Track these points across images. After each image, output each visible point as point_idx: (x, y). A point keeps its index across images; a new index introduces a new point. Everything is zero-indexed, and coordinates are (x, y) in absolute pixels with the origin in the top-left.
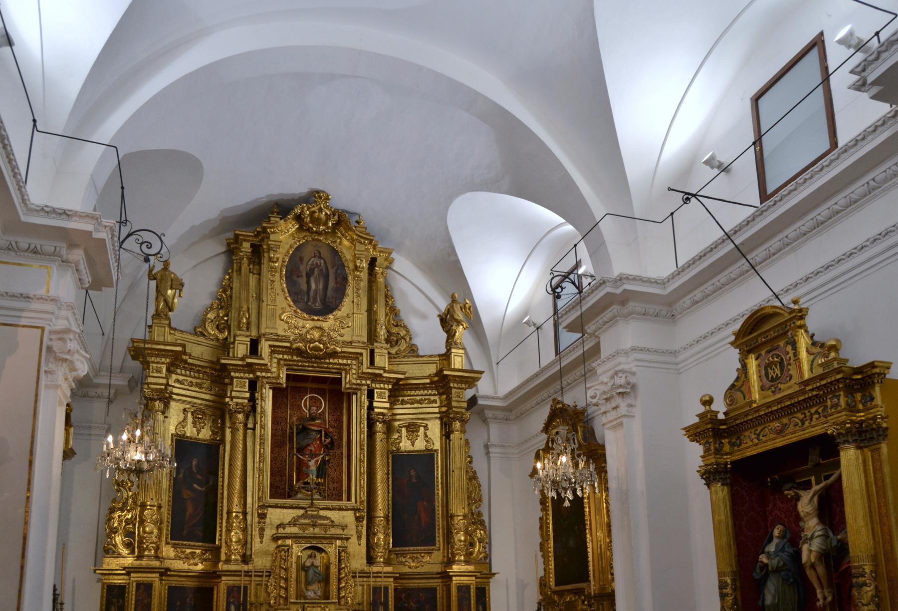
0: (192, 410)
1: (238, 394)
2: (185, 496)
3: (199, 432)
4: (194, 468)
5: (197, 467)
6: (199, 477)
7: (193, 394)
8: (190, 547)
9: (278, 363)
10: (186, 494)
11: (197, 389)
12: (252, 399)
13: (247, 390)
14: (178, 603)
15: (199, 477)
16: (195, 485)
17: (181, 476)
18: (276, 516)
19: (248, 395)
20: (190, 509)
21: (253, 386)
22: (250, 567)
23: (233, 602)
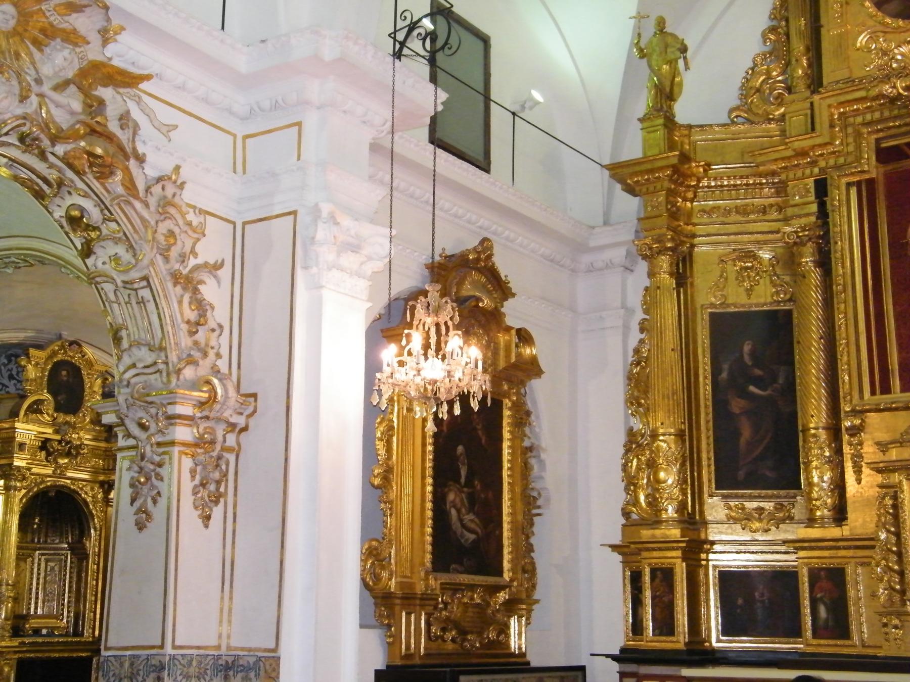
0: (734, 256)
1: (796, 210)
2: (736, 410)
3: (749, 292)
4: (747, 358)
5: (753, 354)
6: (758, 372)
7: (733, 228)
8: (751, 498)
9: (858, 135)
10: (737, 405)
11: (739, 218)
12: (823, 213)
13: (813, 198)
14: (740, 601)
15: (758, 372)
16: (752, 388)
17: (724, 375)
18: (879, 427)
19: (814, 208)
20: (746, 433)
21: (822, 188)
22: (845, 531)
23: (821, 599)
